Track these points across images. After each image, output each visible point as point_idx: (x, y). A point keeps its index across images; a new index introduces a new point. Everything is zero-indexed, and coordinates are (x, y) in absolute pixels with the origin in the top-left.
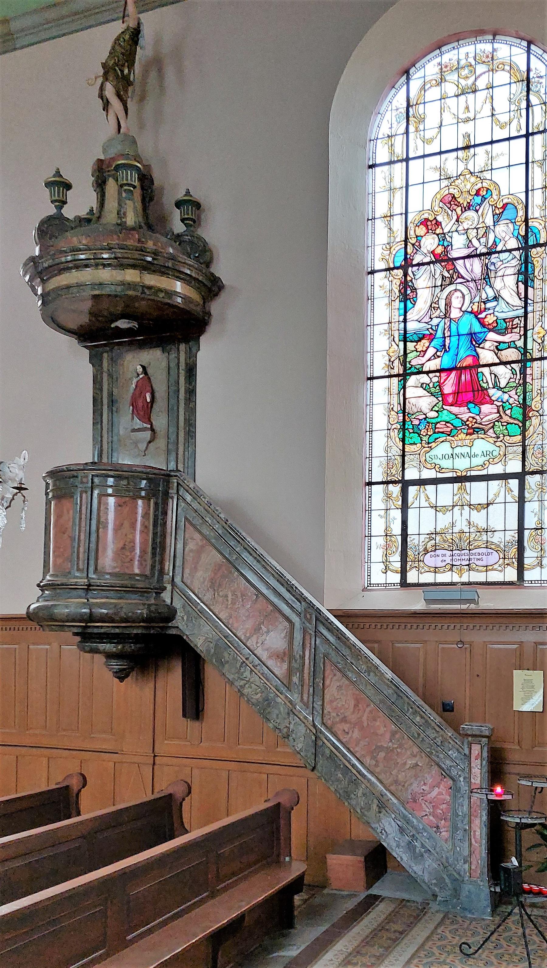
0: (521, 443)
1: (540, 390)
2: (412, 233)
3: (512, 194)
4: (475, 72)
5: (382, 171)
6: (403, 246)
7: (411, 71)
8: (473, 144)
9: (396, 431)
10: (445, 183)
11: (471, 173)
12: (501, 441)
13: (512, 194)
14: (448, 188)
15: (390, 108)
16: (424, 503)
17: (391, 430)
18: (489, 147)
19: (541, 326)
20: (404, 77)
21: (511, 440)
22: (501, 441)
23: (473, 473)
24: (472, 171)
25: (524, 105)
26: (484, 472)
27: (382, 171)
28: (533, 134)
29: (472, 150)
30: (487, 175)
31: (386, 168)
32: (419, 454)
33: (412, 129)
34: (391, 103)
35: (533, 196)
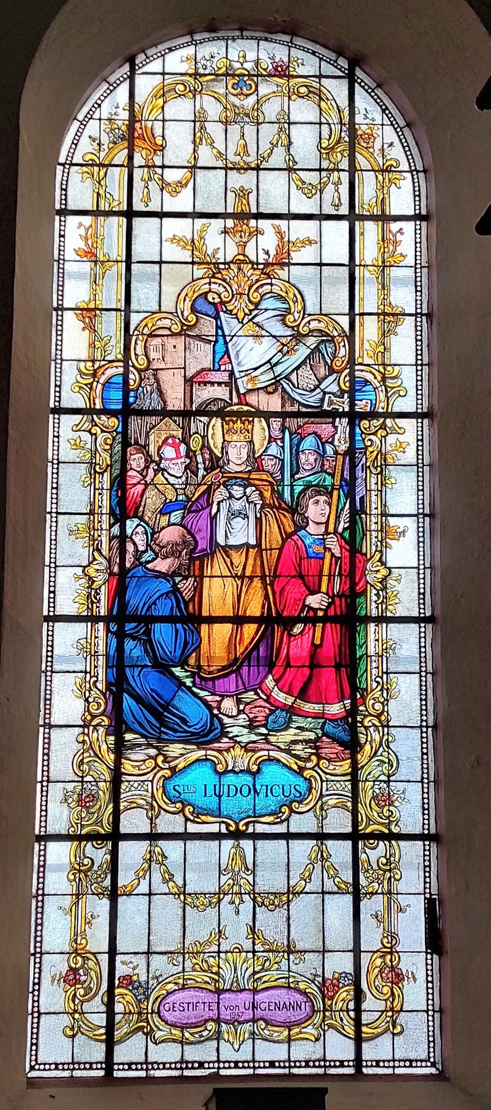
0: (349, 778)
1: (382, 678)
2: (140, 350)
3: (325, 315)
4: (256, 90)
5: (80, 225)
6: (121, 370)
7: (140, 58)
8: (254, 210)
9: (101, 730)
10: (199, 272)
11: (252, 263)
12: (312, 769)
13: (325, 315)
14: (208, 280)
15: (96, 116)
16: (159, 886)
17: (91, 728)
18: (283, 224)
19: (380, 560)
20: (126, 68)
21: (331, 767)
22: (312, 769)
23: (260, 829)
24: (253, 258)
25: (345, 164)
26: (281, 829)
27: (80, 225)
28: (363, 218)
29: (253, 223)
30: (283, 273)
31: (87, 220)
32: (152, 781)
33: (138, 160)
34: (99, 106)
35: (362, 325)
